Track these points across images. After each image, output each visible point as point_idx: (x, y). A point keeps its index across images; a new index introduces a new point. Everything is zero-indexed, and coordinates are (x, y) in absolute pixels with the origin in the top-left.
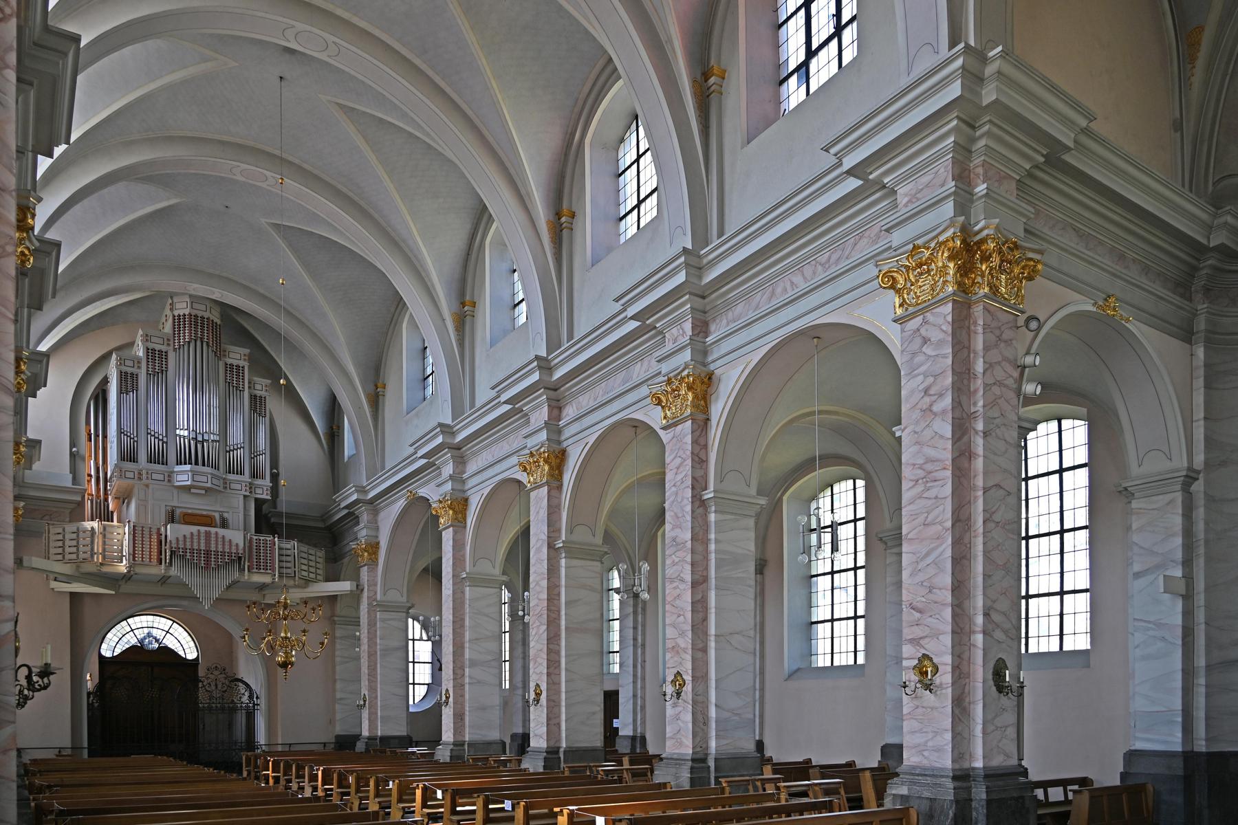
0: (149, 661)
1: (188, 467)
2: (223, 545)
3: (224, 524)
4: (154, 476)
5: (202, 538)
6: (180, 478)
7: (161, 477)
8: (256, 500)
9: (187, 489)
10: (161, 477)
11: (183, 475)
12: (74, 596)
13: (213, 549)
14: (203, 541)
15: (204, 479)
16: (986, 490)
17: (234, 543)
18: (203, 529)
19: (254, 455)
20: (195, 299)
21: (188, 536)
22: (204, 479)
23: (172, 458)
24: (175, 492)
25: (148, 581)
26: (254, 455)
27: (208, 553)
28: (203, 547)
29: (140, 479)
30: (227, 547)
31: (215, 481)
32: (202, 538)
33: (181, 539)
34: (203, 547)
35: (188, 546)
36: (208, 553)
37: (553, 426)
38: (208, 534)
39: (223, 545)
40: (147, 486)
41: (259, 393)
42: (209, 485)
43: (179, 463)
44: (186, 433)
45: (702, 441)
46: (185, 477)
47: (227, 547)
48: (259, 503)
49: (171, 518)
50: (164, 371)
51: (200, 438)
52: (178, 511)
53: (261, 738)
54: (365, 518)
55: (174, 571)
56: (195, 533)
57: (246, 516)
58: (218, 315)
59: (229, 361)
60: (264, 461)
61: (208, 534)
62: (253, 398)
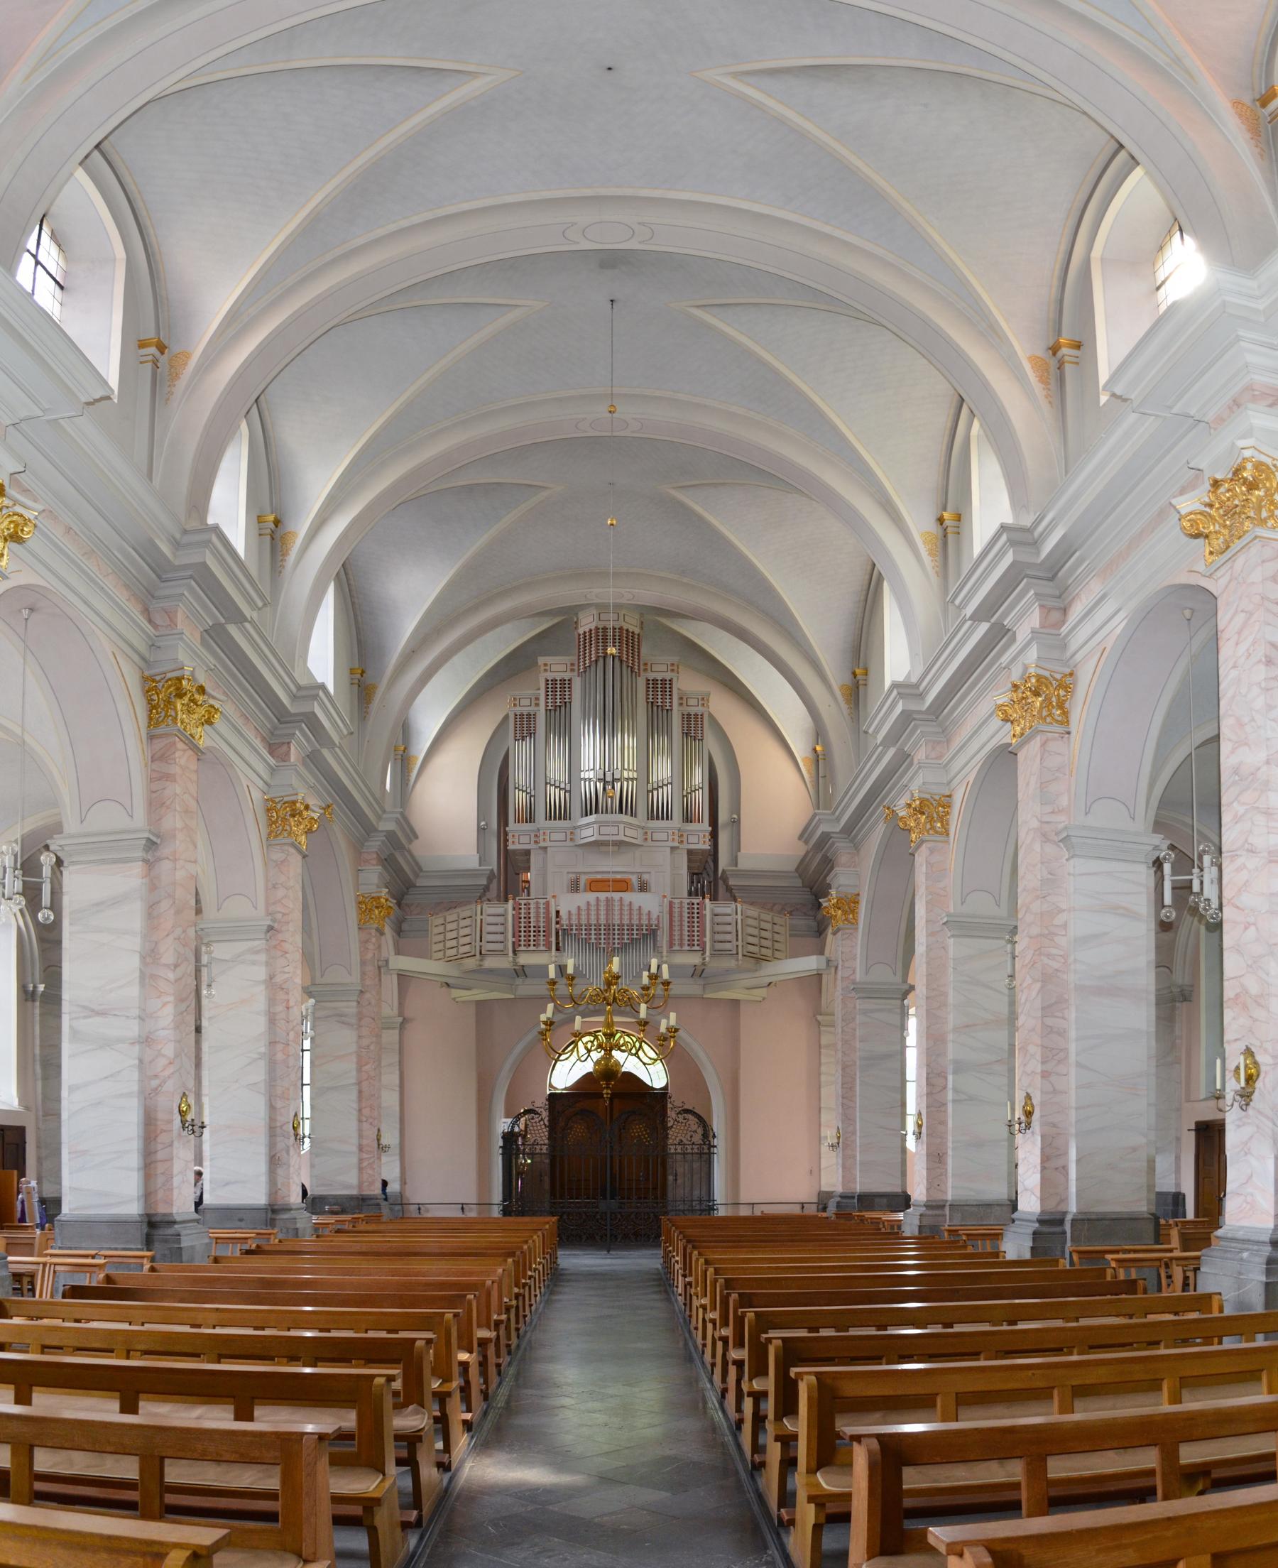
0: (610, 1088)
2: (631, 914)
3: (643, 887)
4: (554, 837)
5: (602, 908)
6: (587, 832)
7: (561, 836)
8: (690, 852)
10: (561, 836)
12: (479, 1004)
14: (603, 912)
15: (614, 830)
17: (645, 911)
18: (603, 896)
20: (602, 608)
21: (584, 907)
22: (614, 830)
23: (576, 809)
28: (603, 921)
30: (635, 917)
31: (628, 832)
32: (602, 908)
33: (574, 911)
35: (584, 921)
36: (608, 927)
39: (631, 914)
42: (621, 837)
44: (591, 775)
47: (635, 917)
49: (574, 887)
50: (567, 704)
51: (609, 778)
52: (583, 879)
53: (719, 1194)
54: (843, 858)
56: (593, 902)
58: (634, 622)
59: (651, 676)
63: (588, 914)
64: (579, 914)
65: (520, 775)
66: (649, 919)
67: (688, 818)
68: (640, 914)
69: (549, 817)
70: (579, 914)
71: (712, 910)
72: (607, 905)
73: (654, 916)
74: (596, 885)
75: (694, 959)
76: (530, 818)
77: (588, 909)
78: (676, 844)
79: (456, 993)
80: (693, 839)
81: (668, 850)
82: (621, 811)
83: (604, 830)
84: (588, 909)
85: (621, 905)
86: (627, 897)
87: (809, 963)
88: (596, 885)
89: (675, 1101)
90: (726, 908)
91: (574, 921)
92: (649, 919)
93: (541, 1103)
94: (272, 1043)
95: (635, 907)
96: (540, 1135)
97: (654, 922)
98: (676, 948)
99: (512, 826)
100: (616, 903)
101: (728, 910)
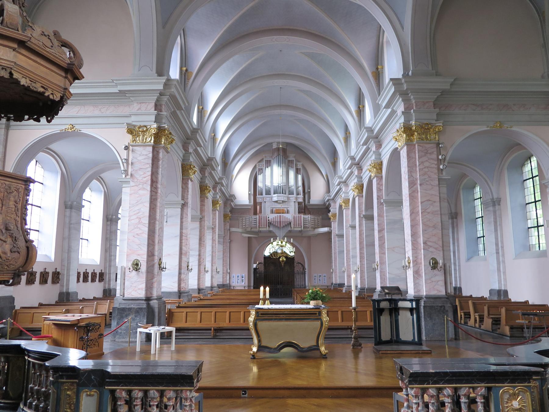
1: (276, 195)
3: (288, 212)
9: (276, 202)
11: (275, 197)
12: (249, 237)
16: (421, 203)
18: (279, 215)
19: (297, 188)
23: (272, 192)
25: (265, 232)
26: (297, 188)
36: (280, 222)
37: (360, 177)
38: (280, 216)
43: (274, 194)
45: (381, 183)
48: (299, 203)
49: (272, 212)
55: (271, 229)
57: (295, 208)
60: (301, 189)
61: (280, 216)
65: (260, 184)
67: (298, 194)
74: (278, 212)
76: (262, 194)
79: (243, 235)
83: (279, 198)
86: (284, 215)
87: (325, 229)
88: (278, 212)
89: (296, 260)
90: (306, 216)
93: (262, 260)
94: (212, 252)
96: (262, 268)
99: (258, 196)
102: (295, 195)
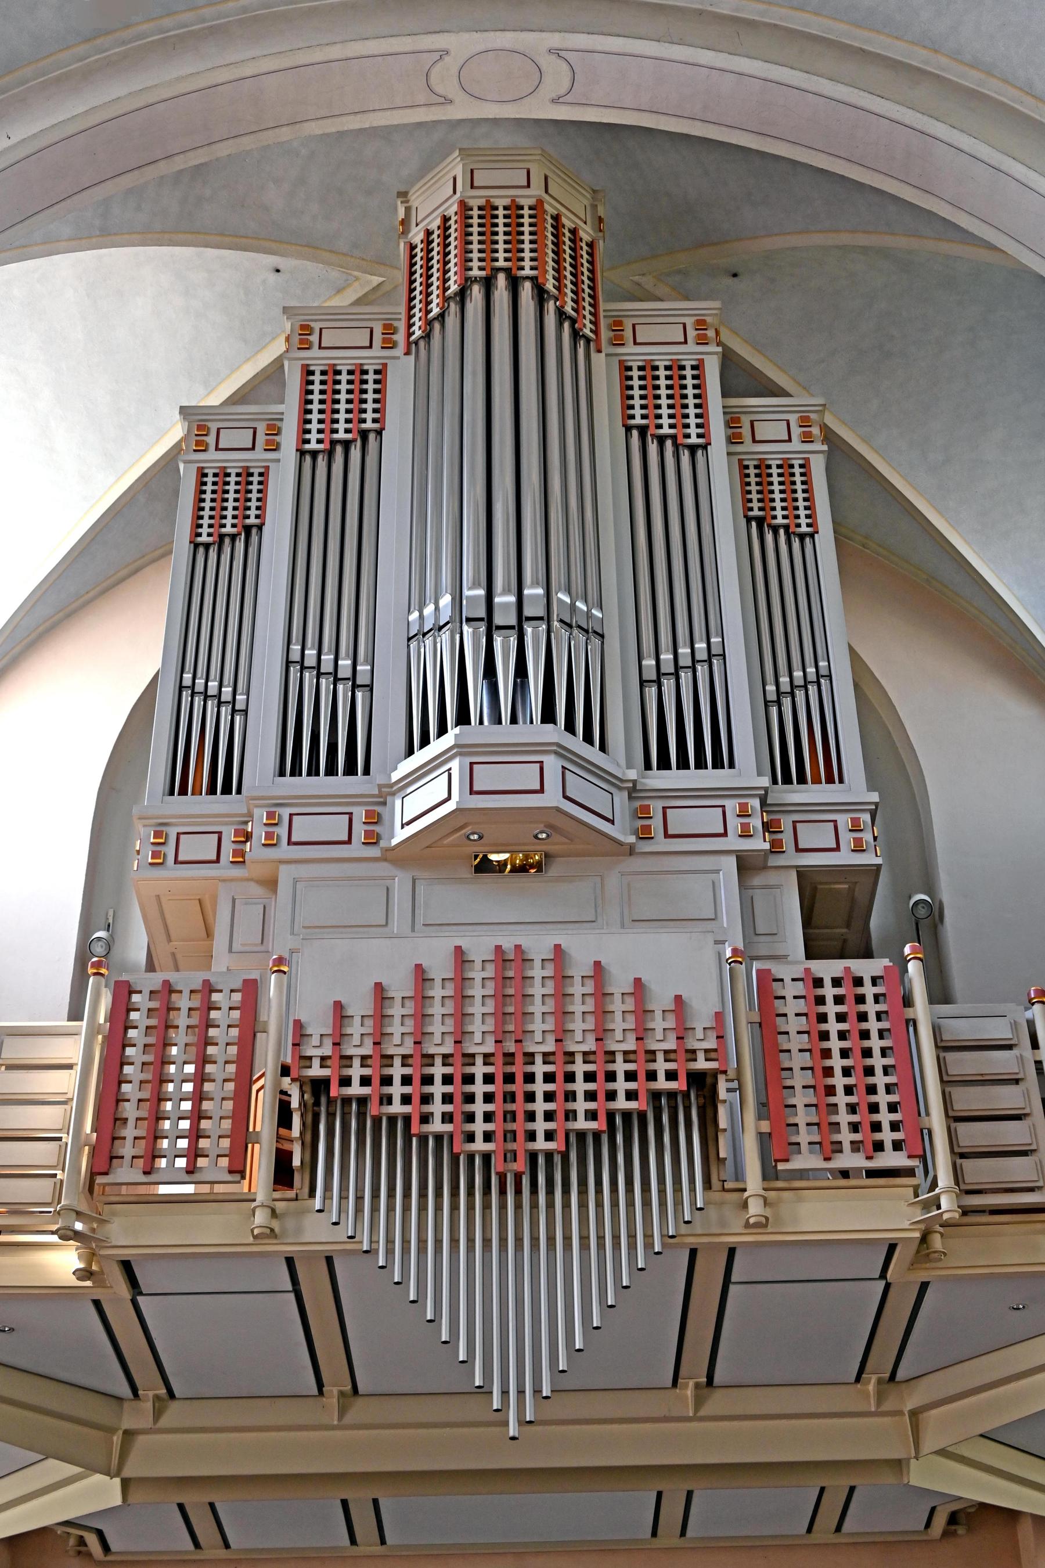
2: (602, 1013)
13: (540, 1040)
17: (660, 999)
21: (400, 986)
24: (400, 882)
27: (511, 1071)
29: (240, 859)
33: (359, 1006)
34: (480, 1042)
36: (511, 1071)
40: (271, 884)
41: (773, 453)
42: (552, 798)
46: (433, 790)
47: (618, 1024)
56: (440, 968)
62: (753, 476)
63: (422, 1017)
64: (381, 1017)
66: (682, 1032)
68: (642, 1013)
69: (290, 765)
70: (381, 1017)
71: (936, 1031)
72: (502, 980)
73: (701, 1017)
75: (892, 1214)
77: (421, 998)
78: (759, 844)
80: (814, 836)
81: (731, 862)
82: (548, 716)
84: (421, 998)
85: (561, 978)
91: (358, 1046)
92: (682, 1032)
95: (620, 983)
97: (702, 1041)
98: (806, 1160)
100: (537, 972)
101: (999, 1031)
102: (748, 770)
